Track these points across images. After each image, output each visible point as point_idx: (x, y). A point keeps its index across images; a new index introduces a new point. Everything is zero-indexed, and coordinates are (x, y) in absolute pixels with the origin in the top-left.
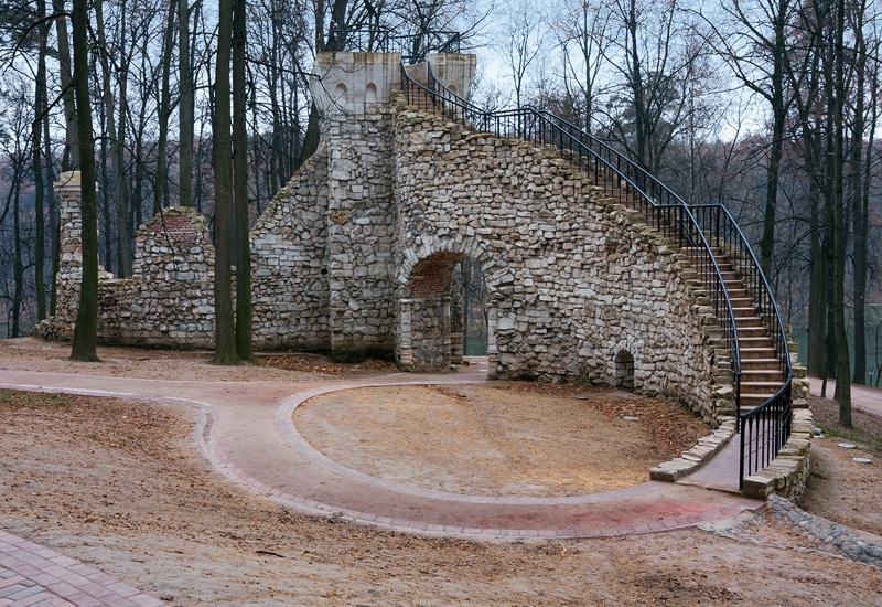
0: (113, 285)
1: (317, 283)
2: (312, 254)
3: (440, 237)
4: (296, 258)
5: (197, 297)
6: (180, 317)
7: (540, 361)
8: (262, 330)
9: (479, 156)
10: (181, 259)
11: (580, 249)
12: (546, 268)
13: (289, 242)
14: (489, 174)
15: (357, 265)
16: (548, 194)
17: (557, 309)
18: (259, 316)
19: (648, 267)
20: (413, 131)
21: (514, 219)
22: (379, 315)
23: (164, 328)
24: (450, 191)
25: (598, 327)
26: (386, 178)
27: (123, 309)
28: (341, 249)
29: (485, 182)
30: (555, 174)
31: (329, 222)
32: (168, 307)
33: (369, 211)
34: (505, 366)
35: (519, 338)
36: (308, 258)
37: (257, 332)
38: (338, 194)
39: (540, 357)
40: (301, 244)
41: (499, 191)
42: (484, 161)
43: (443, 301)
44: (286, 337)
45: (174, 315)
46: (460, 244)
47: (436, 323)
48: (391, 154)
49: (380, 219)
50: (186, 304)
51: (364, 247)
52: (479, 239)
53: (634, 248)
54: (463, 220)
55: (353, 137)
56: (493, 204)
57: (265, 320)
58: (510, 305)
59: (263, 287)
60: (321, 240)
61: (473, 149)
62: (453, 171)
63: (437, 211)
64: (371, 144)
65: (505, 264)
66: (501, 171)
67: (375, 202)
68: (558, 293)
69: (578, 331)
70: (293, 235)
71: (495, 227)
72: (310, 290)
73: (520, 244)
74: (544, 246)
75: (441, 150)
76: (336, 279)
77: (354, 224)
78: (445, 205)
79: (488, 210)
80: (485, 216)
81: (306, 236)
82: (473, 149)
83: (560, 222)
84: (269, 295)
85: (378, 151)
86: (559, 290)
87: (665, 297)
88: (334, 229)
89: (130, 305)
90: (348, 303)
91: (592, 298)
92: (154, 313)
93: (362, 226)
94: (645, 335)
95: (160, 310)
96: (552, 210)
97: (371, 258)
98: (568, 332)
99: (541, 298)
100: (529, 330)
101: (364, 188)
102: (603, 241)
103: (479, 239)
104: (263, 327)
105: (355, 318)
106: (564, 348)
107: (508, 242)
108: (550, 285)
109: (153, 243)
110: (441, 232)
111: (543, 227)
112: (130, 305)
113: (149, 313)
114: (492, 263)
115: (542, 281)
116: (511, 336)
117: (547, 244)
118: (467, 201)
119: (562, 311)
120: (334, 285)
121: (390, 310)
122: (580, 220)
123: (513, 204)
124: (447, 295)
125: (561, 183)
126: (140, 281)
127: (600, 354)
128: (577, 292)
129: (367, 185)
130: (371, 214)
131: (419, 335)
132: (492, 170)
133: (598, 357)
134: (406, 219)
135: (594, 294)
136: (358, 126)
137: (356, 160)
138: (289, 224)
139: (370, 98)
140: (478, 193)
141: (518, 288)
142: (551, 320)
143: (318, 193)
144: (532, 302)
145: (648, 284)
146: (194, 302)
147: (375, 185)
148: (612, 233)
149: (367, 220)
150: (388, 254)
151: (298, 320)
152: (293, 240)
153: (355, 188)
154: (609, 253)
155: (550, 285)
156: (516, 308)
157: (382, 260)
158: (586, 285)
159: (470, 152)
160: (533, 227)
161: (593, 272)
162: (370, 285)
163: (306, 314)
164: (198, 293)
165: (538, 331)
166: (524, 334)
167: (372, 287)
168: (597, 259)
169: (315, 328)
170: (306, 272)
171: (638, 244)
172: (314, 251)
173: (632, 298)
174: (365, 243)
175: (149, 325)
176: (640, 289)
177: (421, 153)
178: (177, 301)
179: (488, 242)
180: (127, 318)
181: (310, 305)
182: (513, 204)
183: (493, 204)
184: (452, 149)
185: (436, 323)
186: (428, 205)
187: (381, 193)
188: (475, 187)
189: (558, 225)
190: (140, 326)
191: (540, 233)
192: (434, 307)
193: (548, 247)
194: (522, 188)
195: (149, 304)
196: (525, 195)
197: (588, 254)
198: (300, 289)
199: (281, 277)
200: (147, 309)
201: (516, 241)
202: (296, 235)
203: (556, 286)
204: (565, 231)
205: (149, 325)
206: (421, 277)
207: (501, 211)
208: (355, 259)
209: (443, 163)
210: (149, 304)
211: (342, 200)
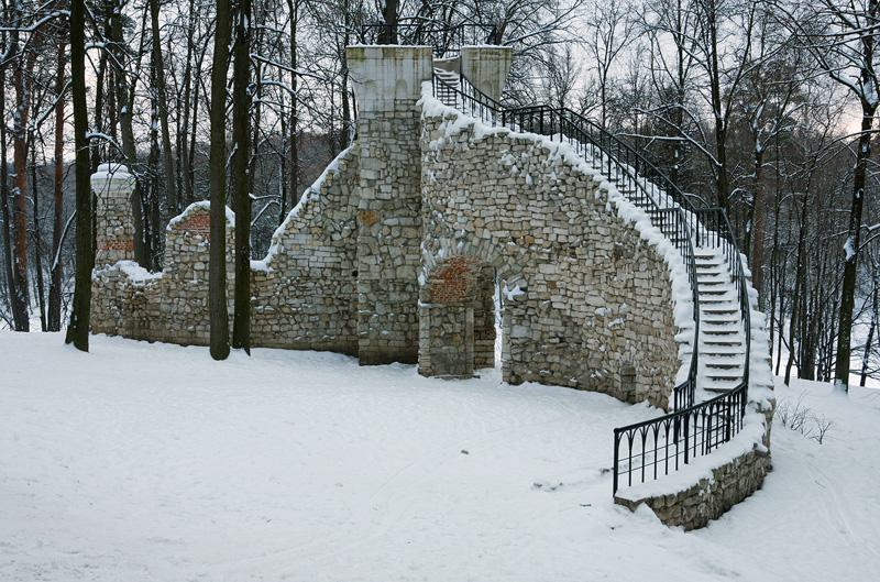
2: (342, 255)
8: (290, 333)
11: (591, 254)
19: (647, 275)
21: (529, 221)
22: (407, 321)
25: (606, 338)
28: (368, 251)
33: (396, 213)
36: (339, 260)
38: (367, 194)
44: (314, 340)
48: (418, 152)
49: (410, 221)
53: (637, 255)
57: (292, 322)
60: (353, 242)
63: (454, 212)
64: (400, 143)
67: (405, 204)
68: (571, 301)
72: (340, 292)
76: (363, 282)
78: (462, 207)
80: (501, 218)
81: (336, 237)
90: (374, 307)
93: (390, 227)
99: (554, 306)
100: (542, 339)
102: (611, 247)
107: (522, 246)
108: (562, 292)
109: (182, 242)
110: (457, 235)
111: (557, 231)
113: (177, 313)
114: (506, 268)
116: (525, 346)
118: (483, 203)
125: (574, 184)
128: (590, 300)
130: (401, 216)
131: (438, 341)
136: (387, 125)
138: (320, 224)
140: (493, 195)
143: (350, 192)
151: (328, 322)
156: (530, 316)
158: (596, 293)
172: (346, 253)
183: (509, 207)
196: (539, 197)
198: (330, 292)
206: (442, 281)
208: (383, 262)
209: (462, 162)
211: (370, 200)
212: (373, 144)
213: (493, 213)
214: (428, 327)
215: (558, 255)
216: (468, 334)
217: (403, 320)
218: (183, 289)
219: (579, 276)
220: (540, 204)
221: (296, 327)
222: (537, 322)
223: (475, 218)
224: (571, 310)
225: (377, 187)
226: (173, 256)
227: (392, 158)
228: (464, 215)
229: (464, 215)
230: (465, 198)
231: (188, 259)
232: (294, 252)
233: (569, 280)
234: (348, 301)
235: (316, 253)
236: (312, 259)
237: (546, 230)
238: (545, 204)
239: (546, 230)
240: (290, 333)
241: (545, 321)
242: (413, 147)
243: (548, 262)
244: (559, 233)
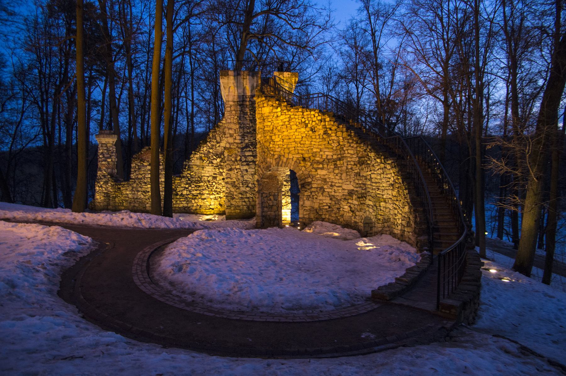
2: (217, 170)
25: (354, 205)
63: (274, 146)
78: (279, 143)
79: (299, 145)
80: (298, 148)
84: (196, 190)
99: (326, 190)
108: (330, 184)
111: (327, 153)
118: (289, 141)
125: (336, 130)
131: (265, 209)
156: (313, 196)
183: (302, 142)
184: (281, 115)
209: (278, 122)
212: (232, 116)
213: (294, 146)
215: (328, 165)
220: (318, 140)
222: (316, 198)
223: (285, 148)
224: (335, 192)
229: (279, 147)
230: (279, 139)
233: (334, 177)
237: (321, 153)
238: (321, 140)
239: (321, 153)
241: (321, 198)
244: (328, 154)
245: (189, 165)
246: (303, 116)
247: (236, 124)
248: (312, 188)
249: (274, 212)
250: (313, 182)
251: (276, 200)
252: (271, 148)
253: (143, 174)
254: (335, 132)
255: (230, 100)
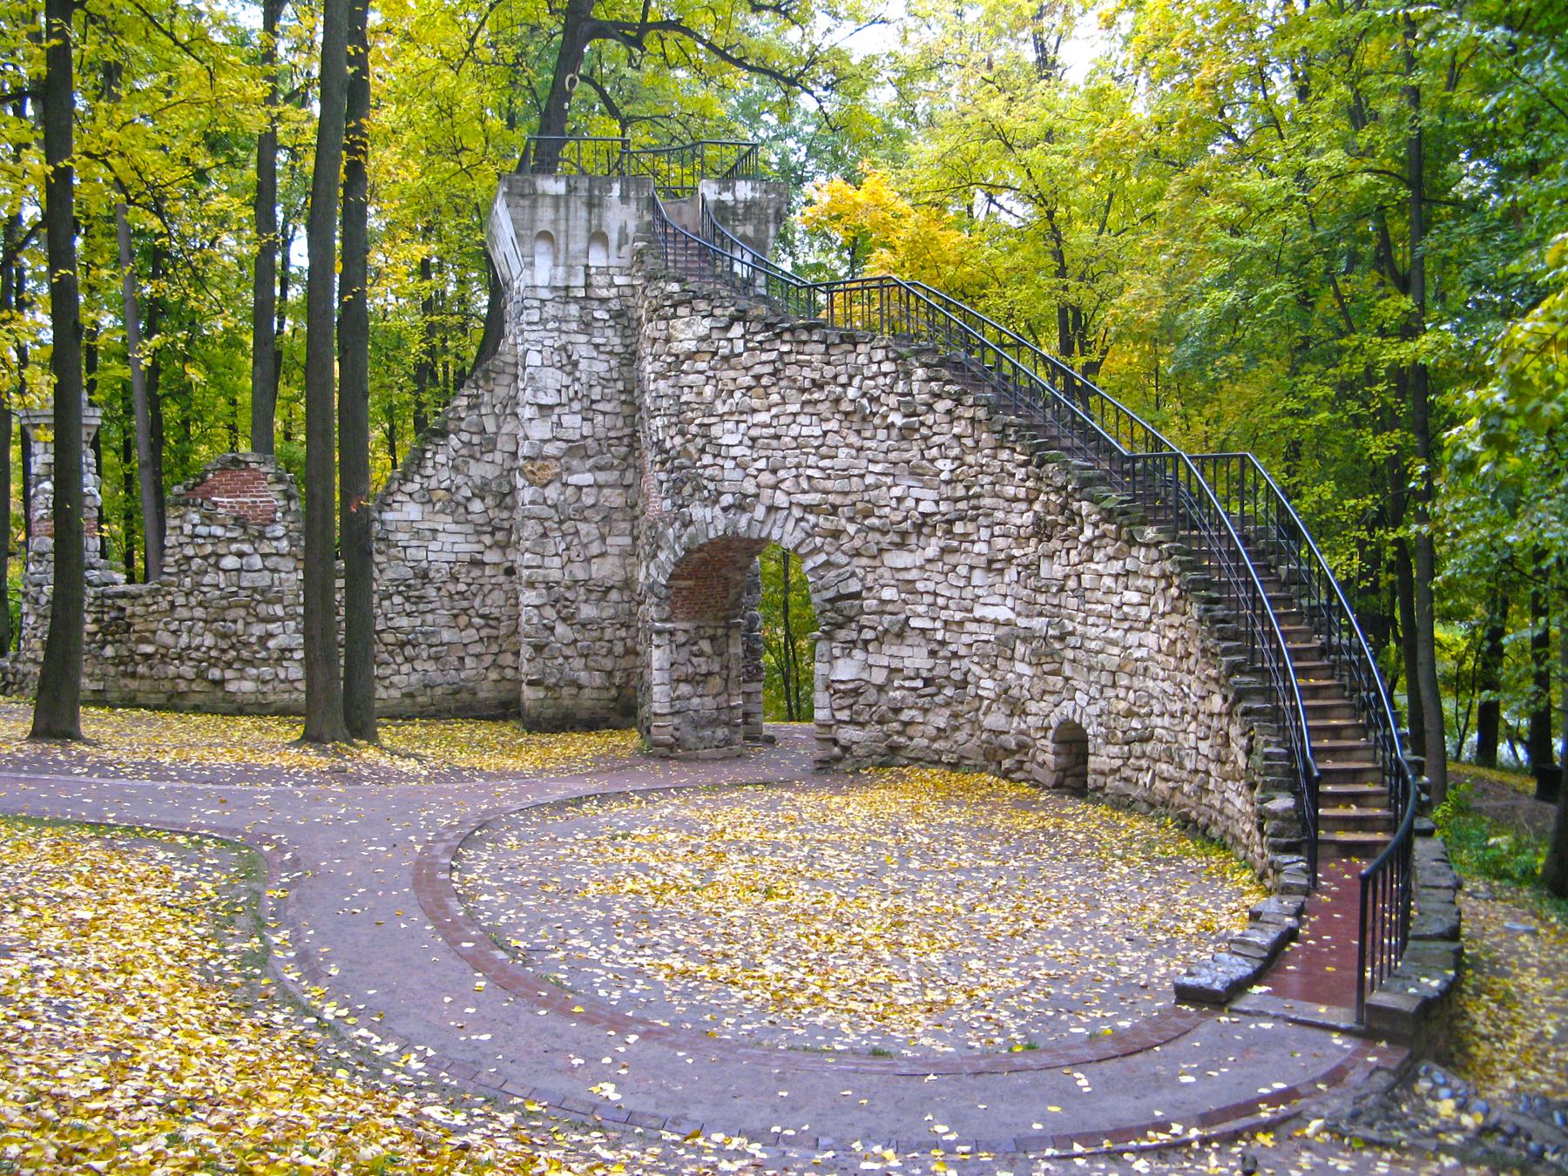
0: (124, 595)
1: (496, 593)
2: (487, 539)
3: (725, 509)
4: (457, 548)
5: (274, 619)
6: (245, 654)
7: (911, 739)
8: (395, 679)
9: (796, 363)
10: (246, 548)
11: (984, 533)
12: (921, 568)
13: (450, 519)
14: (816, 396)
15: (570, 560)
16: (924, 431)
17: (943, 643)
18: (391, 653)
19: (1117, 566)
20: (675, 316)
21: (862, 476)
22: (610, 651)
23: (215, 673)
24: (743, 426)
25: (1020, 676)
26: (624, 402)
27: (143, 640)
28: (540, 530)
29: (808, 409)
30: (938, 396)
31: (520, 482)
32: (225, 636)
33: (591, 462)
34: (846, 749)
35: (872, 695)
36: (479, 547)
37: (387, 683)
38: (539, 430)
39: (910, 731)
40: (467, 522)
41: (833, 425)
42: (807, 372)
43: (728, 627)
45: (237, 651)
46: (762, 522)
47: (716, 668)
50: (258, 630)
51: (583, 527)
52: (797, 513)
53: (1088, 532)
54: (766, 478)
55: (564, 328)
56: (824, 450)
57: (399, 659)
58: (854, 635)
59: (397, 599)
60: (505, 515)
61: (785, 348)
62: (749, 388)
63: (720, 461)
65: (843, 559)
66: (839, 390)
67: (604, 443)
68: (944, 615)
69: (983, 683)
70: (456, 507)
71: (827, 493)
73: (873, 521)
74: (918, 527)
75: (726, 351)
76: (531, 585)
77: (566, 485)
78: (735, 452)
79: (812, 460)
80: (810, 472)
81: (477, 506)
82: (785, 348)
83: (948, 483)
84: (408, 615)
85: (610, 353)
86: (946, 607)
87: (1149, 621)
88: (526, 495)
89: (154, 632)
90: (552, 629)
91: (1008, 623)
92: (198, 649)
93: (580, 488)
94: (1109, 692)
95: (209, 640)
96: (932, 461)
97: (595, 548)
98: (962, 685)
99: (914, 623)
100: (890, 681)
101: (584, 419)
102: (1028, 518)
103: (797, 513)
104: (398, 672)
105: (566, 658)
106: (955, 716)
107: (851, 520)
108: (928, 599)
109: (196, 518)
111: (916, 492)
112: (154, 632)
113: (189, 647)
114: (822, 558)
115: (915, 592)
116: (856, 692)
117: (924, 524)
118: (774, 443)
119: (952, 648)
120: (529, 597)
121: (629, 642)
122: (986, 479)
123: (860, 449)
124: (735, 617)
125: (949, 412)
126: (173, 589)
127: (1023, 726)
128: (979, 612)
129: (590, 414)
131: (684, 689)
132: (821, 387)
133: (1022, 732)
134: (663, 476)
135: (1012, 616)
136: (574, 309)
137: (568, 368)
139: (597, 258)
140: (794, 430)
141: (871, 604)
142: (929, 663)
143: (499, 427)
144: (896, 629)
145: (1116, 600)
146: (271, 627)
147: (604, 413)
148: (1046, 504)
149: (587, 478)
150: (627, 540)
151: (462, 659)
152: (452, 513)
153: (566, 420)
154: (1040, 541)
155: (928, 599)
156: (866, 642)
157: (616, 551)
159: (782, 354)
160: (896, 492)
161: (1011, 574)
162: (593, 596)
163: (478, 649)
164: (279, 610)
165: (907, 684)
166: (881, 689)
167: (599, 600)
168: (1016, 552)
169: (493, 675)
170: (476, 572)
171: (1096, 525)
172: (492, 534)
173: (1084, 623)
174: (585, 520)
175: (188, 670)
176: (1100, 608)
177: (691, 356)
178: (240, 625)
179: (812, 518)
180: (147, 656)
181: (484, 633)
182: (860, 449)
183: (824, 450)
184: (747, 349)
185: (716, 668)
186: (703, 451)
187: (614, 428)
188: (790, 419)
189: (946, 491)
190: (171, 670)
191: (910, 503)
192: (712, 639)
193: (926, 530)
194: (877, 421)
195: (190, 631)
196: (882, 434)
197: (1000, 543)
198: (465, 604)
199: (431, 581)
200: (184, 640)
201: (866, 517)
202: (458, 504)
203: (941, 601)
204: (957, 500)
205: (188, 670)
207: (838, 463)
208: (567, 549)
209: (732, 374)
210: (190, 631)
211: (545, 441)
214: (667, 665)
215: (920, 533)
216: (734, 673)
217: (604, 651)
218: (200, 604)
219: (962, 570)
221: (406, 668)
223: (760, 471)
225: (555, 418)
226: (181, 545)
227: (581, 366)
228: (737, 465)
229: (737, 465)
231: (209, 549)
232: (400, 536)
233: (940, 578)
234: (497, 619)
235: (441, 536)
236: (433, 546)
240: (395, 679)
242: (619, 349)
243: (901, 546)
245: (383, 523)
246: (826, 359)
247: (560, 368)
248: (861, 611)
249: (715, 696)
250: (864, 594)
251: (721, 655)
252: (705, 467)
253: (210, 555)
254: (948, 419)
255: (539, 282)
